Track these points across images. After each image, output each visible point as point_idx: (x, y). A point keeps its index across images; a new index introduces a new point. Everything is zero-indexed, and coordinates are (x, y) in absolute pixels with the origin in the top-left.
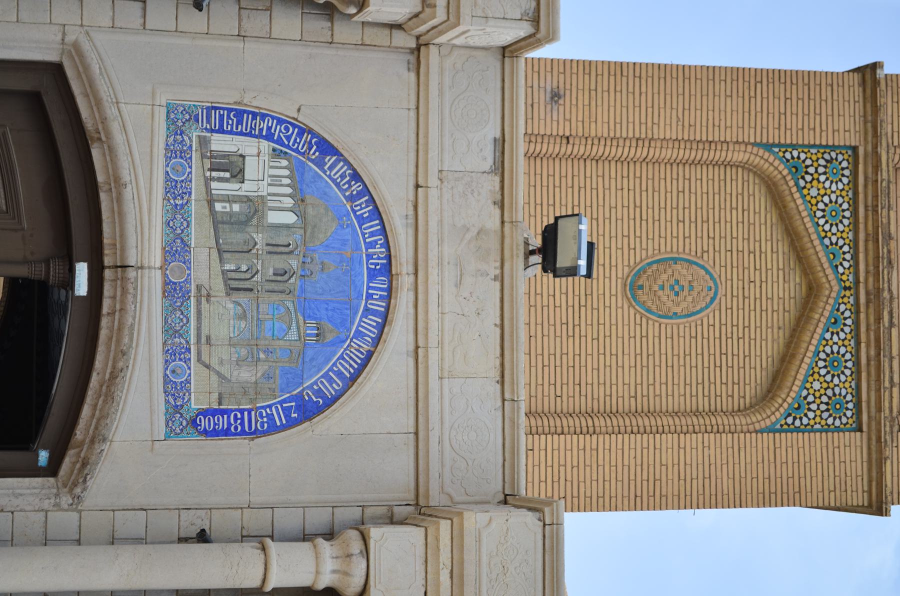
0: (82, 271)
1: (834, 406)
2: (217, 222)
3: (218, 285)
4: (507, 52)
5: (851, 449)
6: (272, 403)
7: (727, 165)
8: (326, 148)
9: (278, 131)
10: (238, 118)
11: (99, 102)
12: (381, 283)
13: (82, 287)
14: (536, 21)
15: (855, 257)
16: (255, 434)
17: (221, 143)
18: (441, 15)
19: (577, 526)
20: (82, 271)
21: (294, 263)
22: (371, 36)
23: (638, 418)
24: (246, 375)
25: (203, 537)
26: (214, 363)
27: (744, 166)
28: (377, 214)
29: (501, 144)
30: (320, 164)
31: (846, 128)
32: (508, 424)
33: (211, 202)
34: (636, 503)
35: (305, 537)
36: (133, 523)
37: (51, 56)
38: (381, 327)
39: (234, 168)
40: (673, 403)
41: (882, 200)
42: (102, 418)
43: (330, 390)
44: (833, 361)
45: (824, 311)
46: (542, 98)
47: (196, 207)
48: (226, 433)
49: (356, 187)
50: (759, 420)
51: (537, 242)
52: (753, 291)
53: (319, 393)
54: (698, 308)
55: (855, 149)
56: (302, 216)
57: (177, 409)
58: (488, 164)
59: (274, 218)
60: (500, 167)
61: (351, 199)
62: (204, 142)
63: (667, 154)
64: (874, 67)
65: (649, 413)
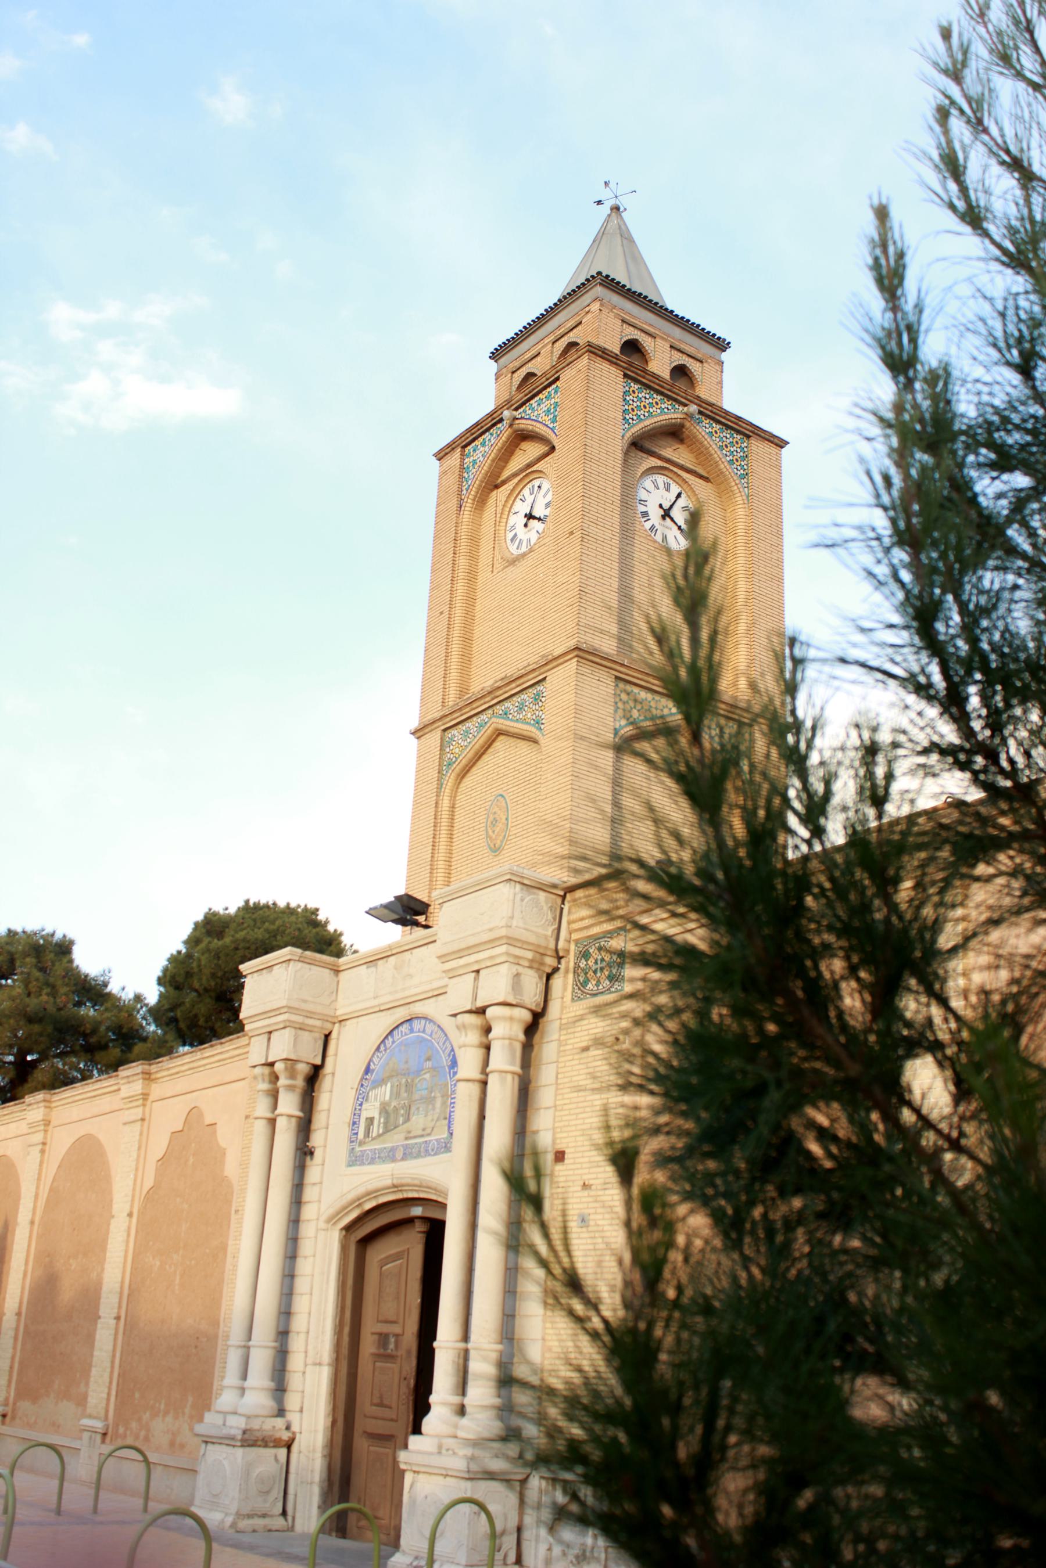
7: (453, 807)
8: (368, 1070)
13: (417, 1211)
24: (438, 1103)
54: (504, 804)
55: (445, 730)
58: (373, 969)
59: (387, 1098)
61: (385, 1050)
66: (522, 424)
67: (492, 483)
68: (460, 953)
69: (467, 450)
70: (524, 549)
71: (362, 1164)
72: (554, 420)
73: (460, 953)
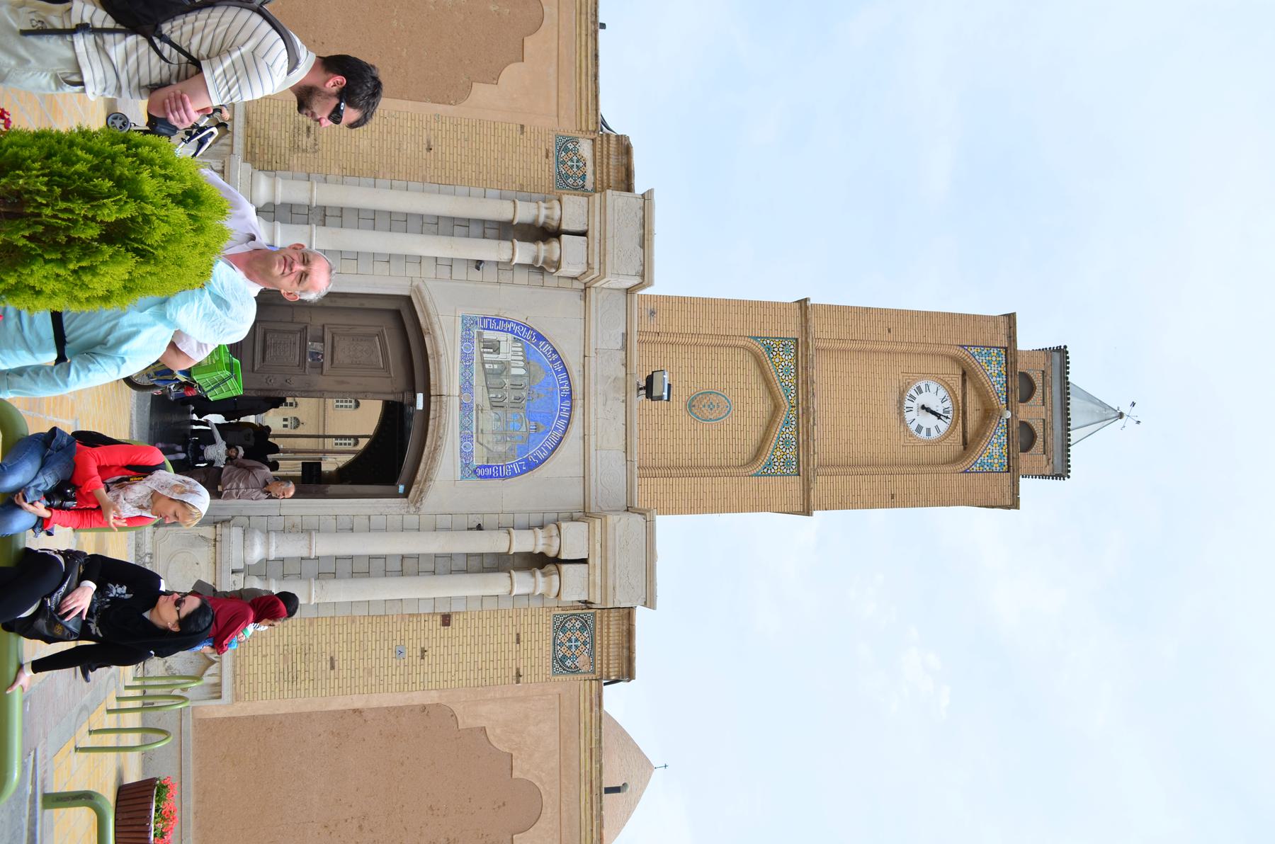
0: (420, 397)
1: (787, 463)
2: (487, 373)
3: (487, 405)
4: (629, 291)
5: (794, 485)
6: (514, 462)
8: (540, 337)
9: (516, 329)
10: (497, 323)
11: (428, 315)
12: (567, 403)
13: (420, 405)
14: (643, 276)
15: (797, 392)
16: (505, 477)
17: (488, 335)
18: (596, 273)
19: (663, 523)
20: (420, 397)
21: (524, 394)
22: (563, 283)
23: (692, 469)
24: (500, 448)
25: (479, 528)
26: (485, 443)
27: (743, 347)
28: (565, 370)
29: (626, 336)
30: (537, 346)
31: (793, 330)
32: (629, 472)
33: (483, 364)
34: (691, 510)
35: (530, 528)
36: (444, 521)
37: (406, 293)
38: (567, 425)
39: (495, 347)
40: (709, 463)
41: (810, 364)
42: (429, 470)
43: (542, 456)
44: (786, 442)
45: (782, 418)
46: (646, 313)
47: (476, 366)
48: (491, 477)
49: (555, 357)
50: (750, 470)
51: (643, 384)
52: (748, 408)
53: (536, 457)
56: (528, 371)
57: (467, 465)
59: (514, 371)
60: (625, 347)
61: (552, 362)
62: (480, 334)
63: (707, 341)
64: (806, 300)
65: (698, 467)
66: (994, 424)
67: (966, 375)
68: (604, 546)
69: (1003, 351)
70: (908, 403)
71: (464, 340)
72: (982, 464)
73: (604, 546)
